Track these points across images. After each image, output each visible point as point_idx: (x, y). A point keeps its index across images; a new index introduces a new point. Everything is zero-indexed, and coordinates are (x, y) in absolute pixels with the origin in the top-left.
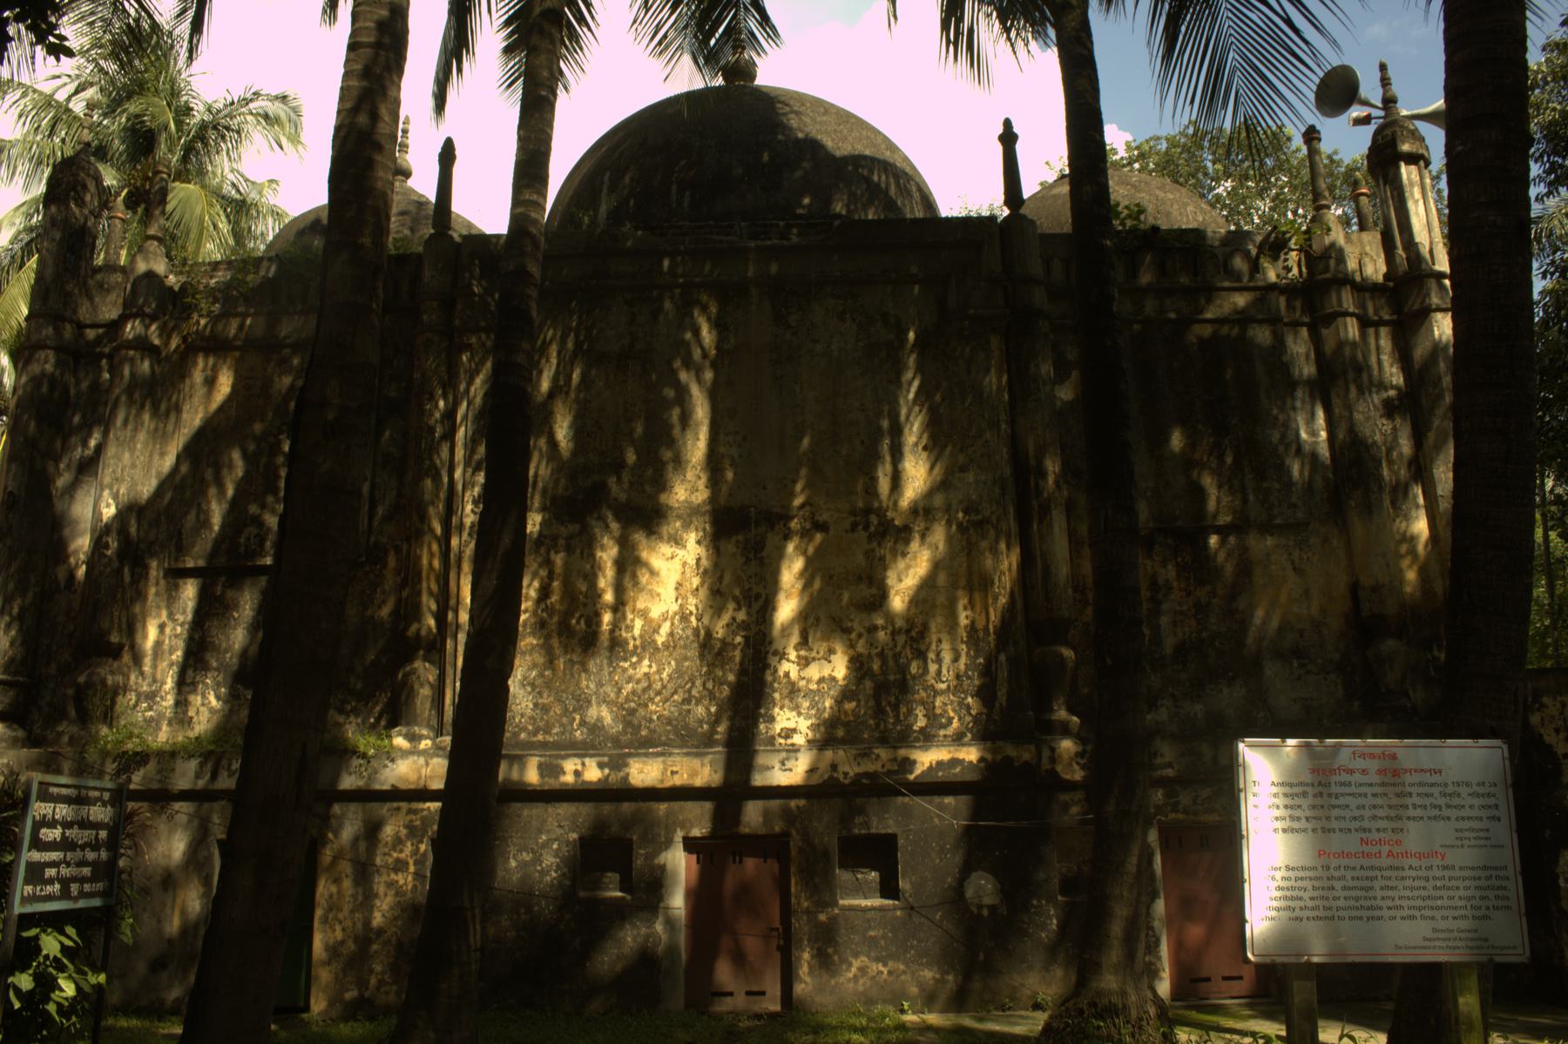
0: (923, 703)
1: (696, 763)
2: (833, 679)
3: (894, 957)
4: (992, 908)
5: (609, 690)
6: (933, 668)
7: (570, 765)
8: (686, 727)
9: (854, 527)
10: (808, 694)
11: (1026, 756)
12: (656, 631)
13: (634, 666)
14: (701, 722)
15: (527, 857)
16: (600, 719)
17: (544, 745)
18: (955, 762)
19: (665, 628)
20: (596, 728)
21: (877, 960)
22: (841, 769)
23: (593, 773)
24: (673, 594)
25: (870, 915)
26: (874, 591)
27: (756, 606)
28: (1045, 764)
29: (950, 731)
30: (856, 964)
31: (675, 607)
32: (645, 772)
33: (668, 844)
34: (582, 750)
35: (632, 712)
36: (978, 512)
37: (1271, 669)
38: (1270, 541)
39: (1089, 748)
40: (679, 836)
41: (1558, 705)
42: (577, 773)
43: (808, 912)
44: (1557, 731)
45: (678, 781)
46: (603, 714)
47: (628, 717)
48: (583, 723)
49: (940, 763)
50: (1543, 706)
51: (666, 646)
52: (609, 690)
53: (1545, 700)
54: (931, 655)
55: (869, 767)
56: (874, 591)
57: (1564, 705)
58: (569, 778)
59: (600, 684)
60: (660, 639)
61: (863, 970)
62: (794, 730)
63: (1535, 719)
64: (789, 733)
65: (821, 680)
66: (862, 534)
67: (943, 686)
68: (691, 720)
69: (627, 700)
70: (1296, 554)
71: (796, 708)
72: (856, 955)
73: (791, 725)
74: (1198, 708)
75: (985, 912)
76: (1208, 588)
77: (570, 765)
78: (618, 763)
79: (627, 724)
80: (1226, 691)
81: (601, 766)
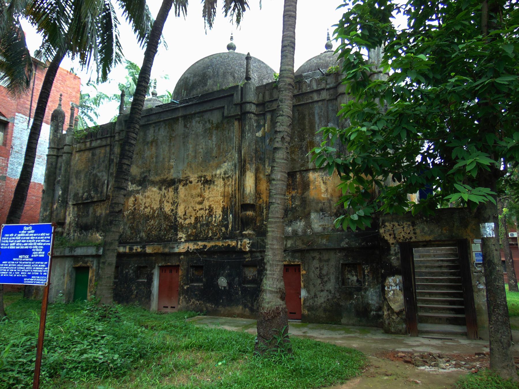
0: (211, 229)
1: (159, 246)
2: (191, 223)
3: (201, 299)
4: (225, 287)
5: (145, 228)
6: (214, 219)
7: (135, 248)
8: (159, 237)
9: (198, 181)
10: (186, 228)
11: (234, 244)
12: (155, 213)
13: (150, 222)
14: (162, 236)
15: (127, 271)
16: (143, 236)
17: (132, 243)
18: (216, 246)
19: (156, 212)
20: (141, 238)
21: (197, 300)
22: (190, 248)
23: (139, 250)
24: (159, 203)
25: (196, 288)
26: (201, 199)
27: (176, 205)
28: (239, 246)
29: (217, 237)
30: (192, 301)
31: (159, 206)
32: (149, 250)
33: (154, 268)
34: (137, 243)
35: (149, 234)
36: (228, 174)
37: (313, 216)
38: (316, 174)
39: (251, 242)
40: (157, 265)
41: (391, 226)
42: (136, 250)
43: (182, 286)
44: (390, 235)
45: (155, 251)
46: (143, 234)
47: (148, 235)
48: (139, 237)
49: (212, 246)
50: (385, 226)
51: (157, 217)
52: (145, 228)
53: (387, 224)
54: (214, 216)
55: (196, 247)
56: (201, 199)
57: (394, 225)
58: (134, 251)
59: (143, 227)
60: (156, 215)
61: (193, 302)
62: (182, 238)
63: (382, 231)
64: (181, 238)
65: (189, 224)
66: (200, 183)
67: (216, 224)
68: (160, 236)
69: (148, 231)
70: (324, 177)
71: (183, 232)
72: (192, 299)
73: (181, 236)
74: (290, 229)
75: (223, 288)
76: (296, 191)
77: (135, 248)
78: (144, 247)
79: (148, 237)
80: (299, 223)
81: (141, 248)
